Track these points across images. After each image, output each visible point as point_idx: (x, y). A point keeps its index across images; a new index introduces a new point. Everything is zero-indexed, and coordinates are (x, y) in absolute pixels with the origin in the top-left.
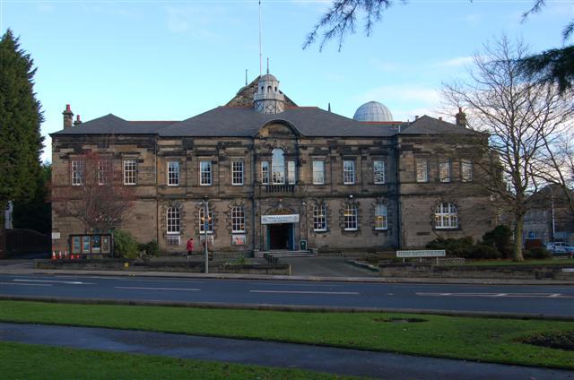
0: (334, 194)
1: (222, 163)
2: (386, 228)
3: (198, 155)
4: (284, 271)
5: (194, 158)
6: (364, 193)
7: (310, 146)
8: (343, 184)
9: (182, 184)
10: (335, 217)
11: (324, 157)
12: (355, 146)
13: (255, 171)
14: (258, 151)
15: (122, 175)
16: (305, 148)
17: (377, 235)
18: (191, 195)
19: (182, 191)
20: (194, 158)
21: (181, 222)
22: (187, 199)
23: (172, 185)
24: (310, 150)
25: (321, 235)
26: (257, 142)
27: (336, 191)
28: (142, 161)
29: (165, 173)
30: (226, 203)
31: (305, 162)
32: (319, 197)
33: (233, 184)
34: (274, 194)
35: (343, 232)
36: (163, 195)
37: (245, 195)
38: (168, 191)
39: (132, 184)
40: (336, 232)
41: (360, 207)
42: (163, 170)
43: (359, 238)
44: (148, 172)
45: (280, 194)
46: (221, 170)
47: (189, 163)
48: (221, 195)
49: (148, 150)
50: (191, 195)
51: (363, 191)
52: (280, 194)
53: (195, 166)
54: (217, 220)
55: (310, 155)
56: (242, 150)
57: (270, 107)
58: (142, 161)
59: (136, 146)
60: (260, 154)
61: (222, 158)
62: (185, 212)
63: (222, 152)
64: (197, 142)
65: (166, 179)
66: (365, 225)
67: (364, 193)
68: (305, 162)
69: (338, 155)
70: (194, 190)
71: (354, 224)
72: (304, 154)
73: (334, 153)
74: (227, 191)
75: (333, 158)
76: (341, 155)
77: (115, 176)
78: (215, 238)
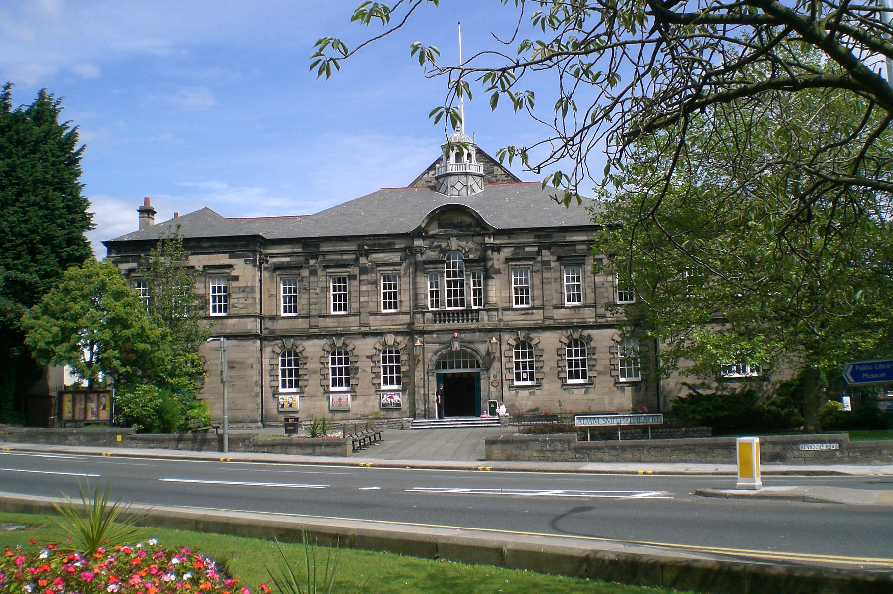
0: (547, 322)
1: (364, 277)
2: (640, 379)
3: (326, 267)
4: (338, 450)
5: (320, 272)
6: (599, 320)
7: (507, 246)
8: (561, 306)
9: (303, 312)
10: (549, 361)
11: (531, 263)
12: (583, 242)
13: (415, 289)
14: (419, 257)
15: (207, 302)
16: (497, 249)
17: (622, 389)
18: (316, 330)
19: (302, 324)
20: (320, 272)
21: (300, 372)
22: (309, 337)
23: (288, 314)
24: (507, 252)
25: (526, 392)
26: (418, 243)
27: (551, 318)
28: (236, 278)
29: (277, 296)
30: (371, 342)
31: (498, 272)
32: (522, 329)
33: (383, 311)
34: (446, 325)
35: (564, 384)
36: (273, 331)
37: (401, 328)
38: (280, 326)
39: (223, 314)
40: (550, 386)
41: (593, 344)
42: (273, 292)
43: (592, 395)
44: (244, 295)
45: (456, 325)
46: (364, 288)
47: (312, 279)
48: (363, 329)
49: (246, 261)
50: (316, 330)
51: (311, 327)
52: (456, 325)
53: (324, 285)
54: (357, 368)
55: (507, 260)
56: (396, 257)
57: (459, 186)
58: (236, 278)
59: (227, 255)
60: (425, 262)
61: (364, 271)
62: (306, 358)
63: (363, 260)
64: (324, 248)
65: (278, 306)
66: (601, 373)
67: (599, 320)
68: (498, 272)
69: (553, 258)
70: (322, 322)
71: (584, 372)
72: (497, 260)
73: (546, 255)
74: (371, 323)
75: (546, 264)
76: (559, 258)
77: (196, 302)
78: (354, 398)
